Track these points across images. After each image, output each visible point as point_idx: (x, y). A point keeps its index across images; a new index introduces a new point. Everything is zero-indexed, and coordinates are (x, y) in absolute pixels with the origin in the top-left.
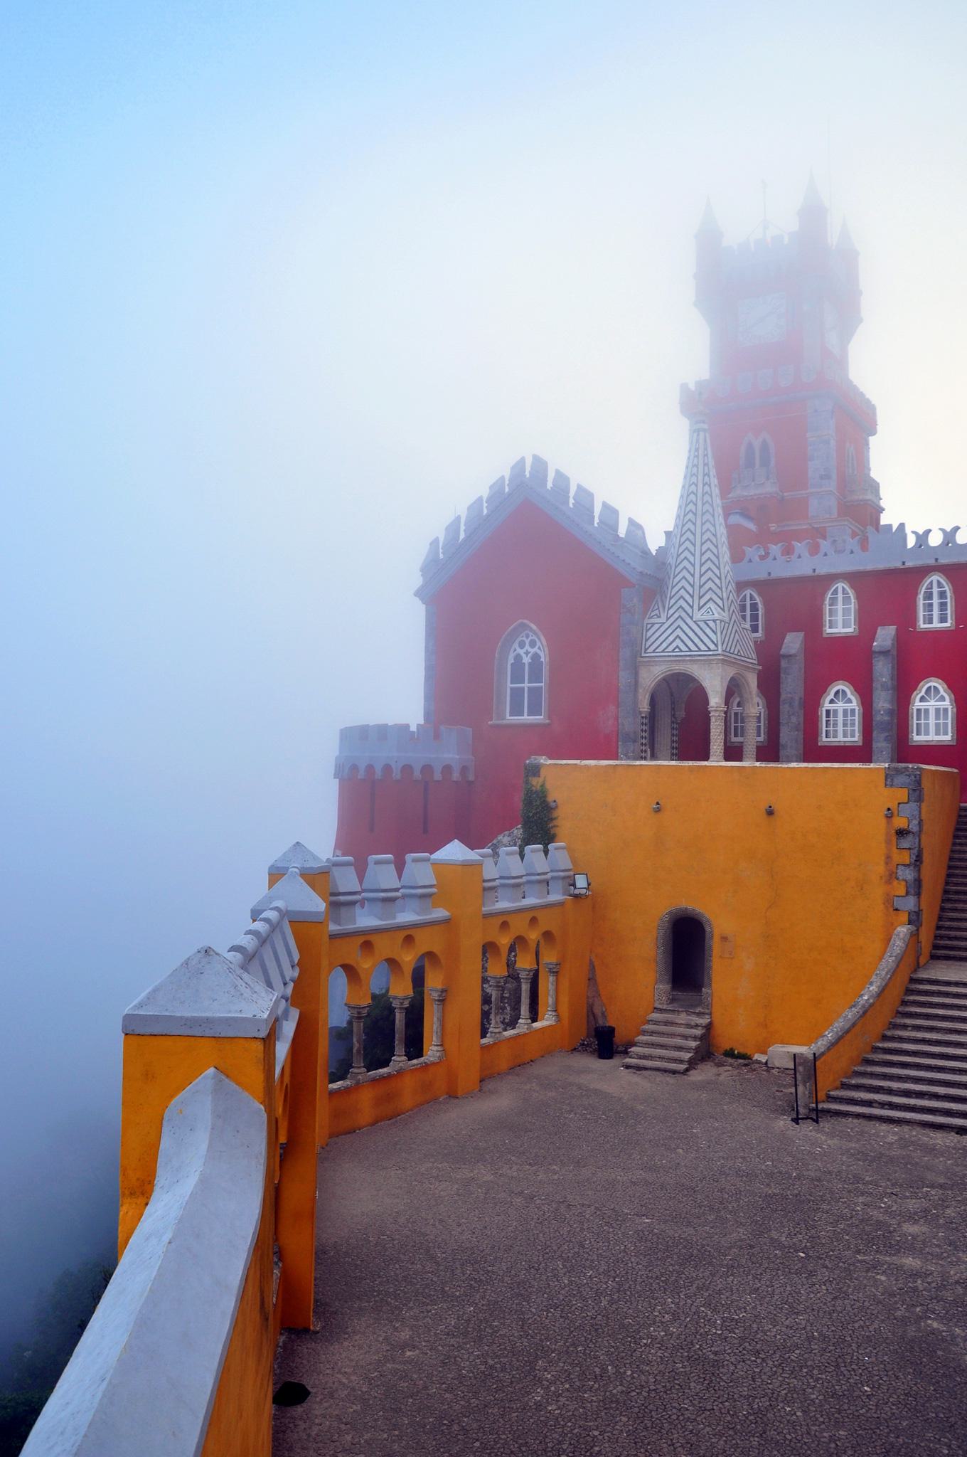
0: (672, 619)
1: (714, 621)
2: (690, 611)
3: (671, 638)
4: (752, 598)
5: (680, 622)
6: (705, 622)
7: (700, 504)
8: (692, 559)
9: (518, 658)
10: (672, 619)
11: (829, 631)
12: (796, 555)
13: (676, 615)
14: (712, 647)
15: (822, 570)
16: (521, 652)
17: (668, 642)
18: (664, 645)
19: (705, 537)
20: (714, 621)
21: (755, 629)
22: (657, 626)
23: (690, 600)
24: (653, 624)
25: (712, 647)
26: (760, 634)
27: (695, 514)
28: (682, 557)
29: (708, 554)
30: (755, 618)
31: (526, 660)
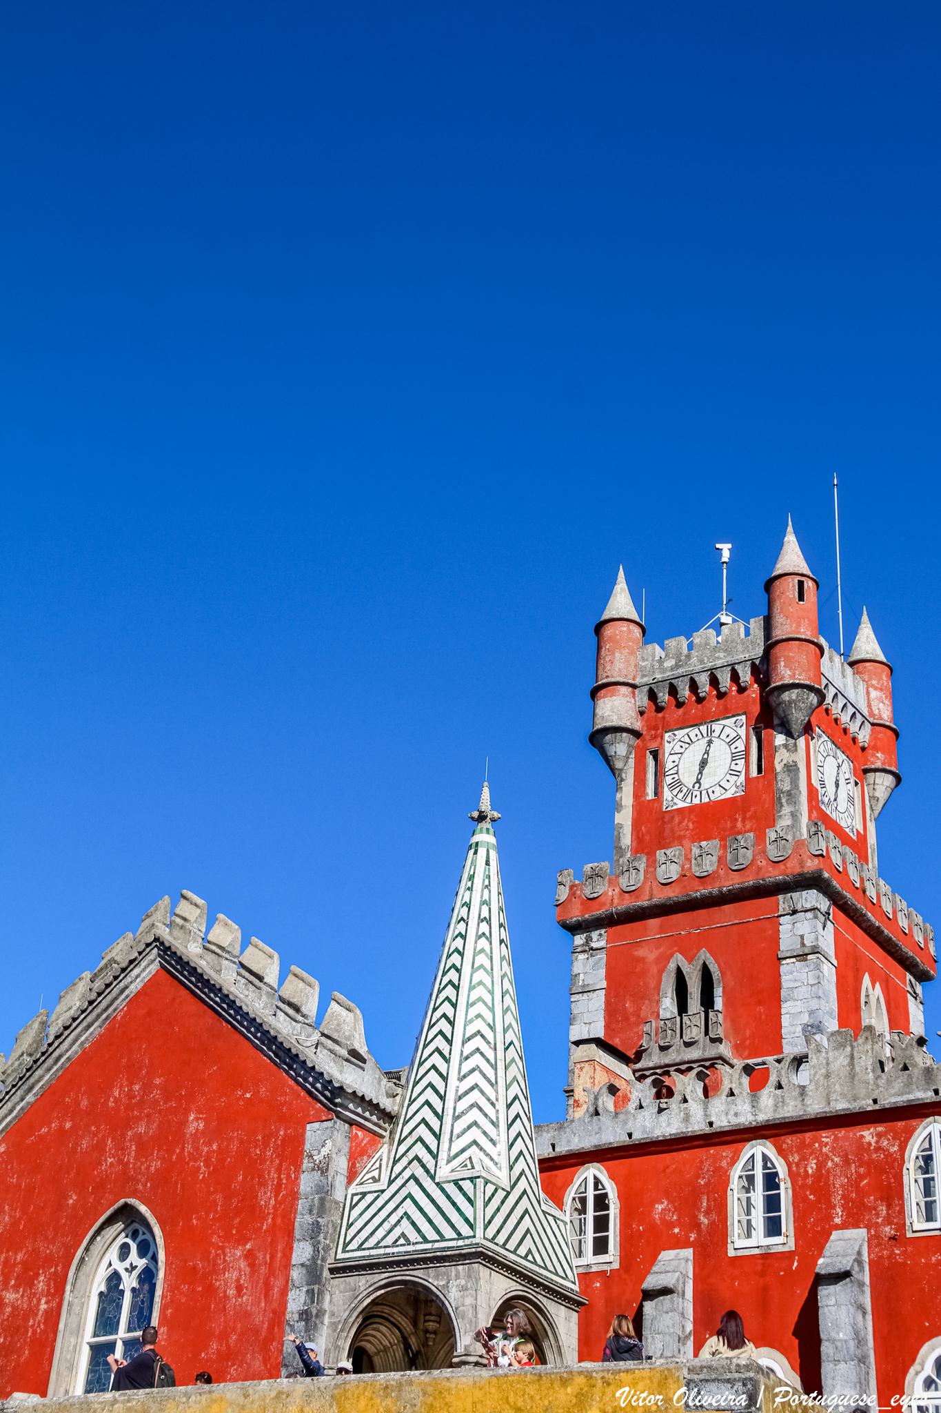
0: (399, 1182)
1: (471, 1179)
2: (431, 1166)
3: (394, 1219)
4: (597, 1182)
5: (412, 1188)
6: (456, 1182)
7: (466, 970)
8: (443, 1067)
9: (114, 1279)
10: (399, 1182)
11: (740, 1243)
12: (677, 1097)
13: (407, 1174)
14: (465, 1230)
15: (722, 1122)
16: (120, 1267)
17: (387, 1226)
18: (380, 1233)
19: (471, 1030)
20: (471, 1179)
21: (601, 1246)
22: (369, 1198)
23: (433, 1144)
24: (364, 1194)
25: (465, 1230)
26: (612, 1257)
27: (457, 988)
28: (427, 1065)
29: (477, 1060)
30: (601, 1224)
31: (129, 1282)
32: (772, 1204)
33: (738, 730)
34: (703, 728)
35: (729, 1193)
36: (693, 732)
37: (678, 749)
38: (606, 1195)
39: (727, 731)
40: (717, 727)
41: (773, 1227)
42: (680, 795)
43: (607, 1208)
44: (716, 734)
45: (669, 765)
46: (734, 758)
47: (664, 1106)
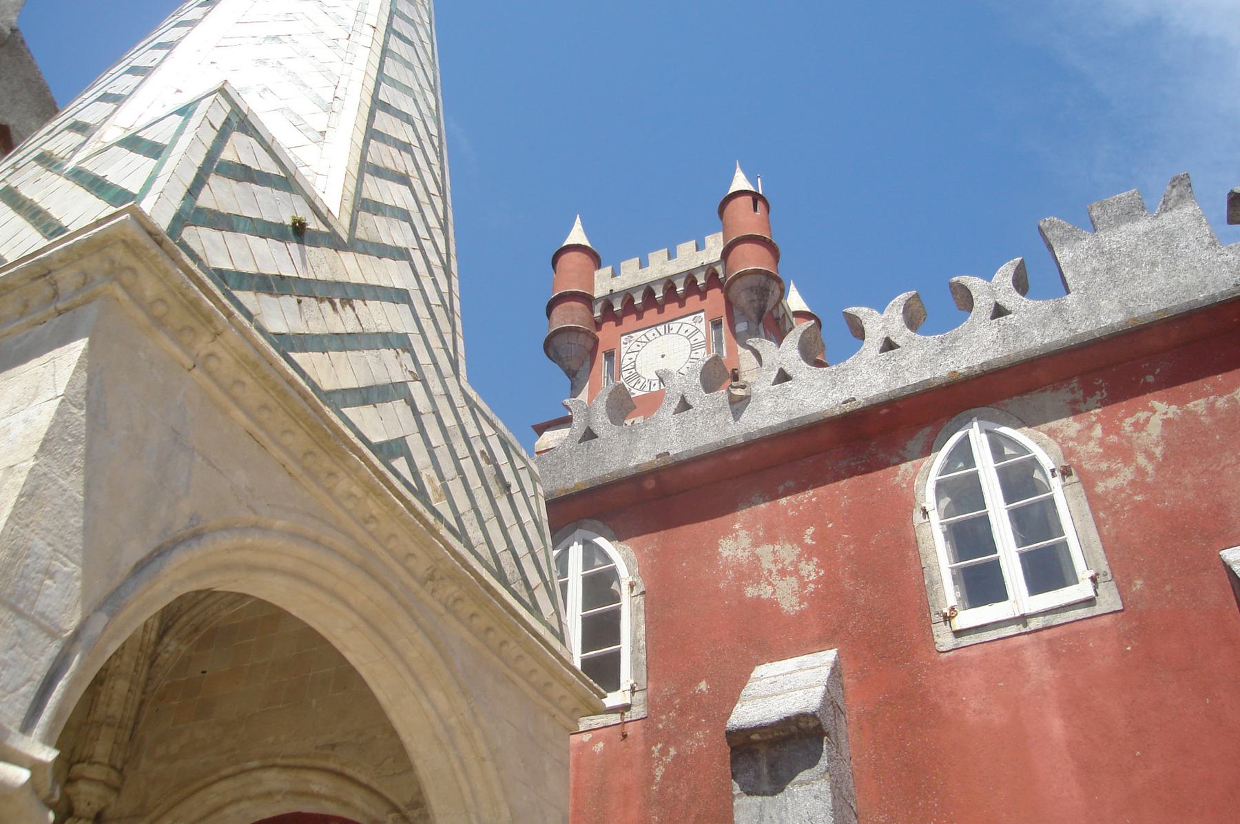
32: (1035, 522)
33: (698, 325)
34: (661, 328)
35: (917, 517)
36: (650, 333)
37: (634, 348)
38: (613, 574)
39: (685, 327)
40: (675, 326)
41: (1047, 570)
42: (638, 386)
43: (616, 598)
44: (675, 331)
45: (625, 362)
46: (693, 348)
47: (739, 392)
